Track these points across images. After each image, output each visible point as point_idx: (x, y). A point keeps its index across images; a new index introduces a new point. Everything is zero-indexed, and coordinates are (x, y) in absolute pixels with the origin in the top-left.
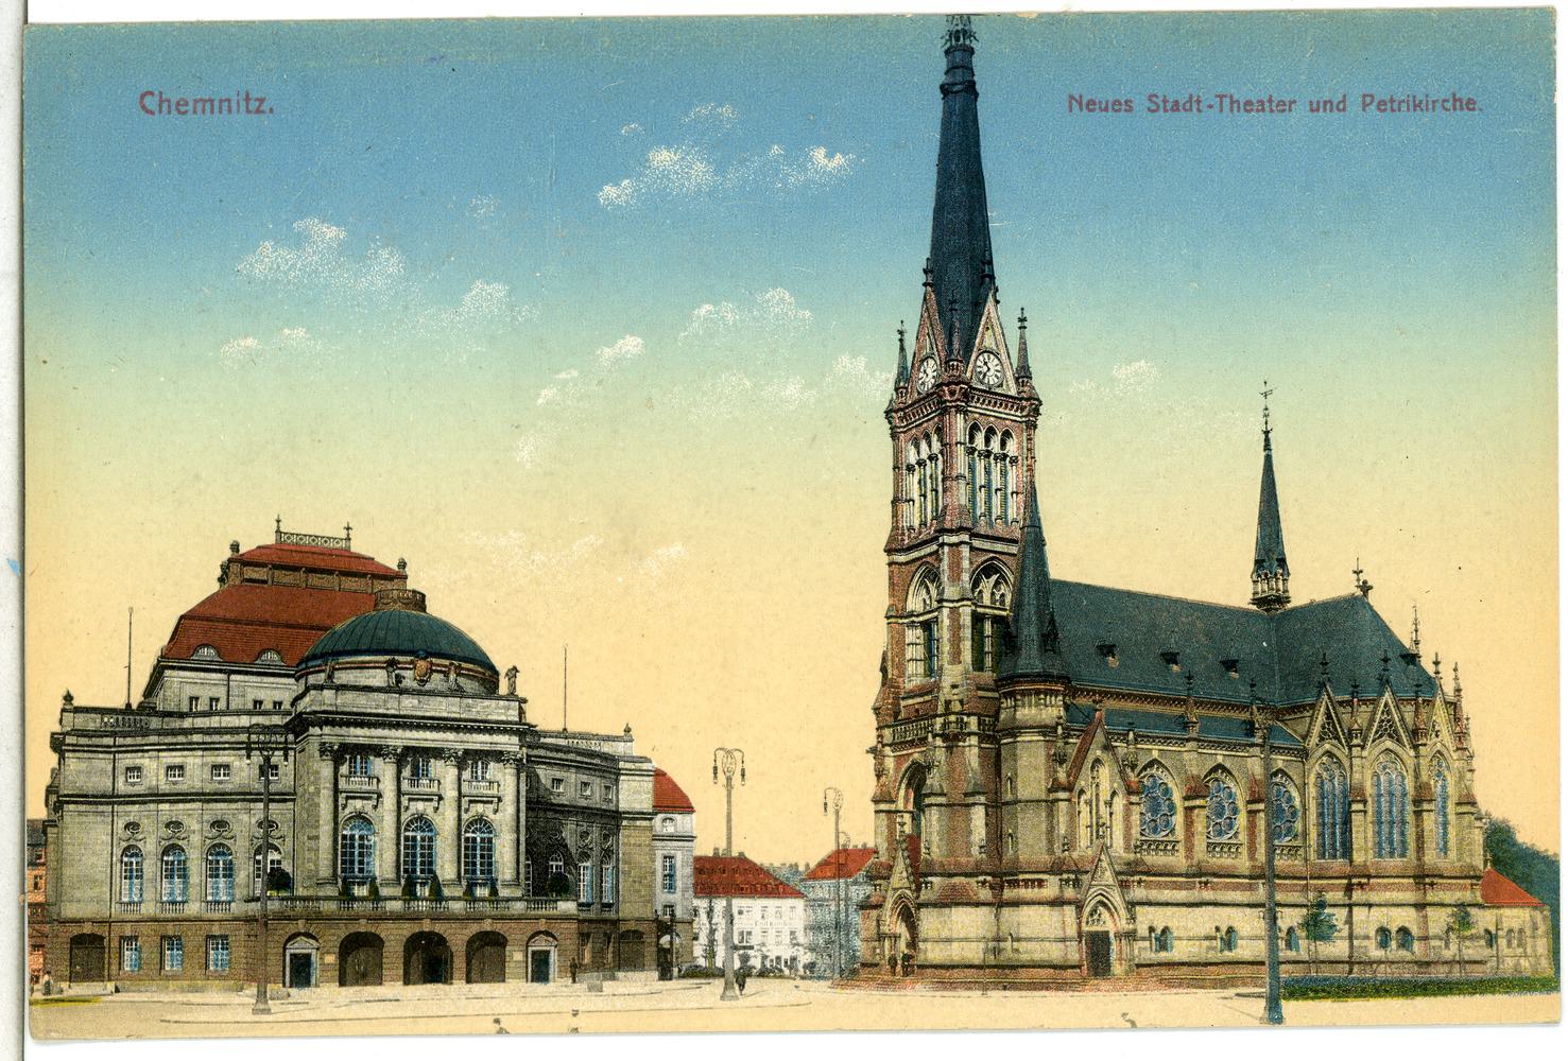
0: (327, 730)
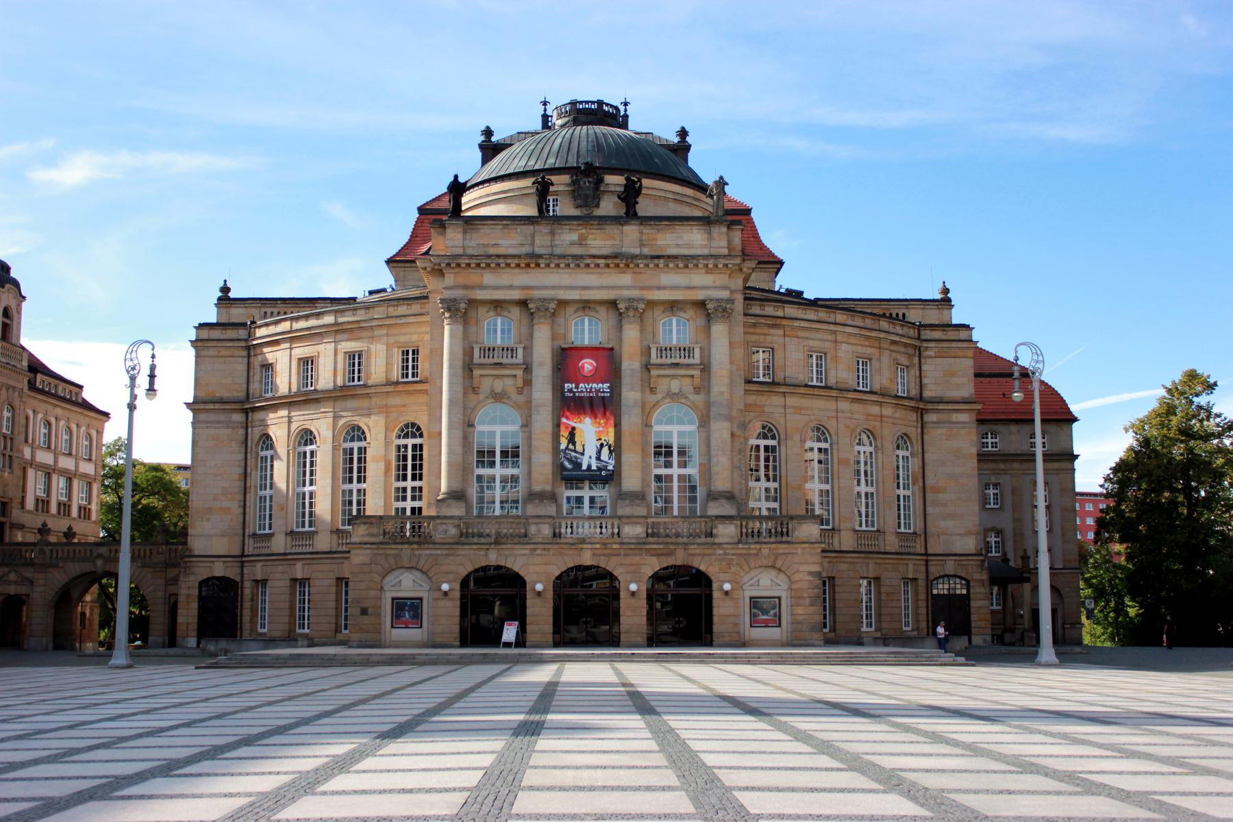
0: (450, 279)
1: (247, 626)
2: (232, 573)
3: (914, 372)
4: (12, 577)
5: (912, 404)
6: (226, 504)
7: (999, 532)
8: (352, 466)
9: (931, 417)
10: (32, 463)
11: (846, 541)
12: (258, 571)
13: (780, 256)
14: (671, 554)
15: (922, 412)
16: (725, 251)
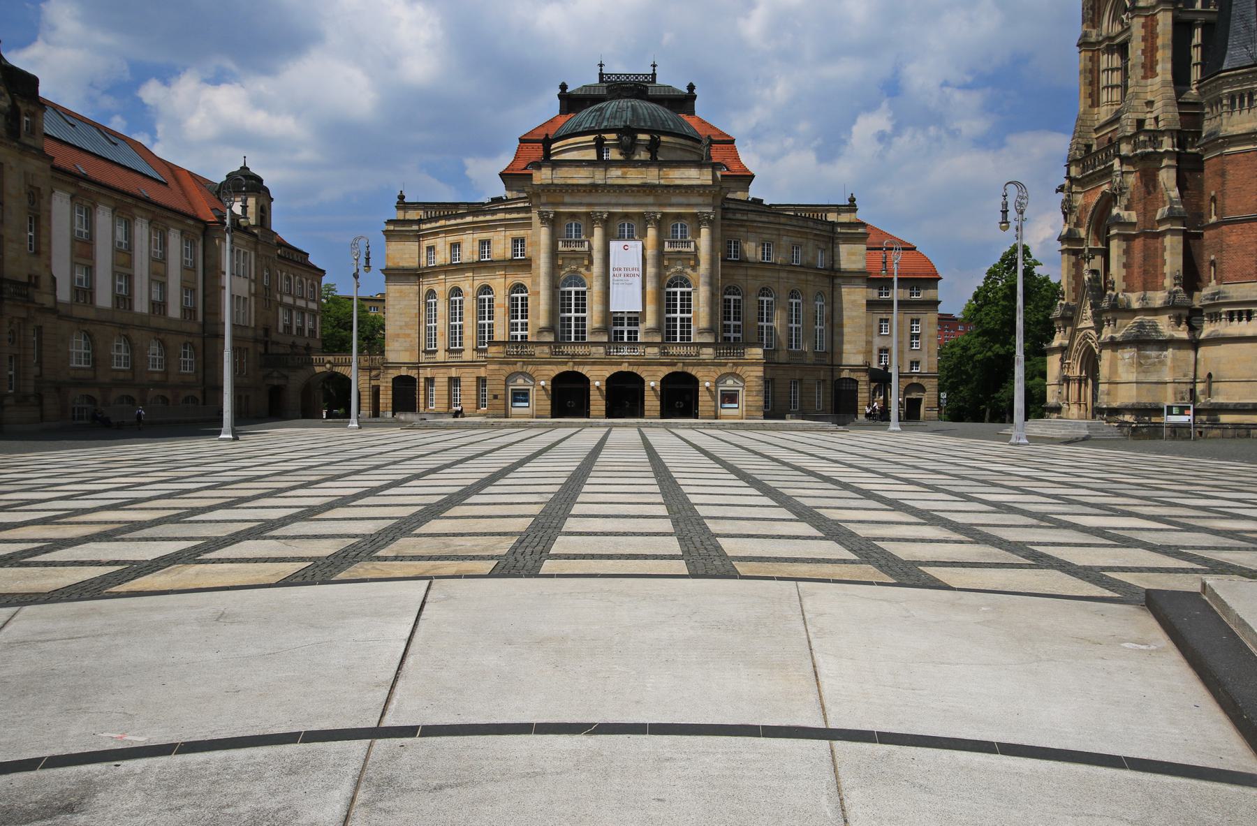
1: (422, 405)
2: (413, 373)
3: (829, 253)
4: (275, 374)
5: (827, 273)
6: (408, 331)
7: (887, 351)
8: (484, 309)
9: (838, 281)
10: (281, 304)
11: (782, 357)
12: (428, 373)
13: (752, 170)
14: (674, 364)
15: (833, 278)
16: (710, 182)
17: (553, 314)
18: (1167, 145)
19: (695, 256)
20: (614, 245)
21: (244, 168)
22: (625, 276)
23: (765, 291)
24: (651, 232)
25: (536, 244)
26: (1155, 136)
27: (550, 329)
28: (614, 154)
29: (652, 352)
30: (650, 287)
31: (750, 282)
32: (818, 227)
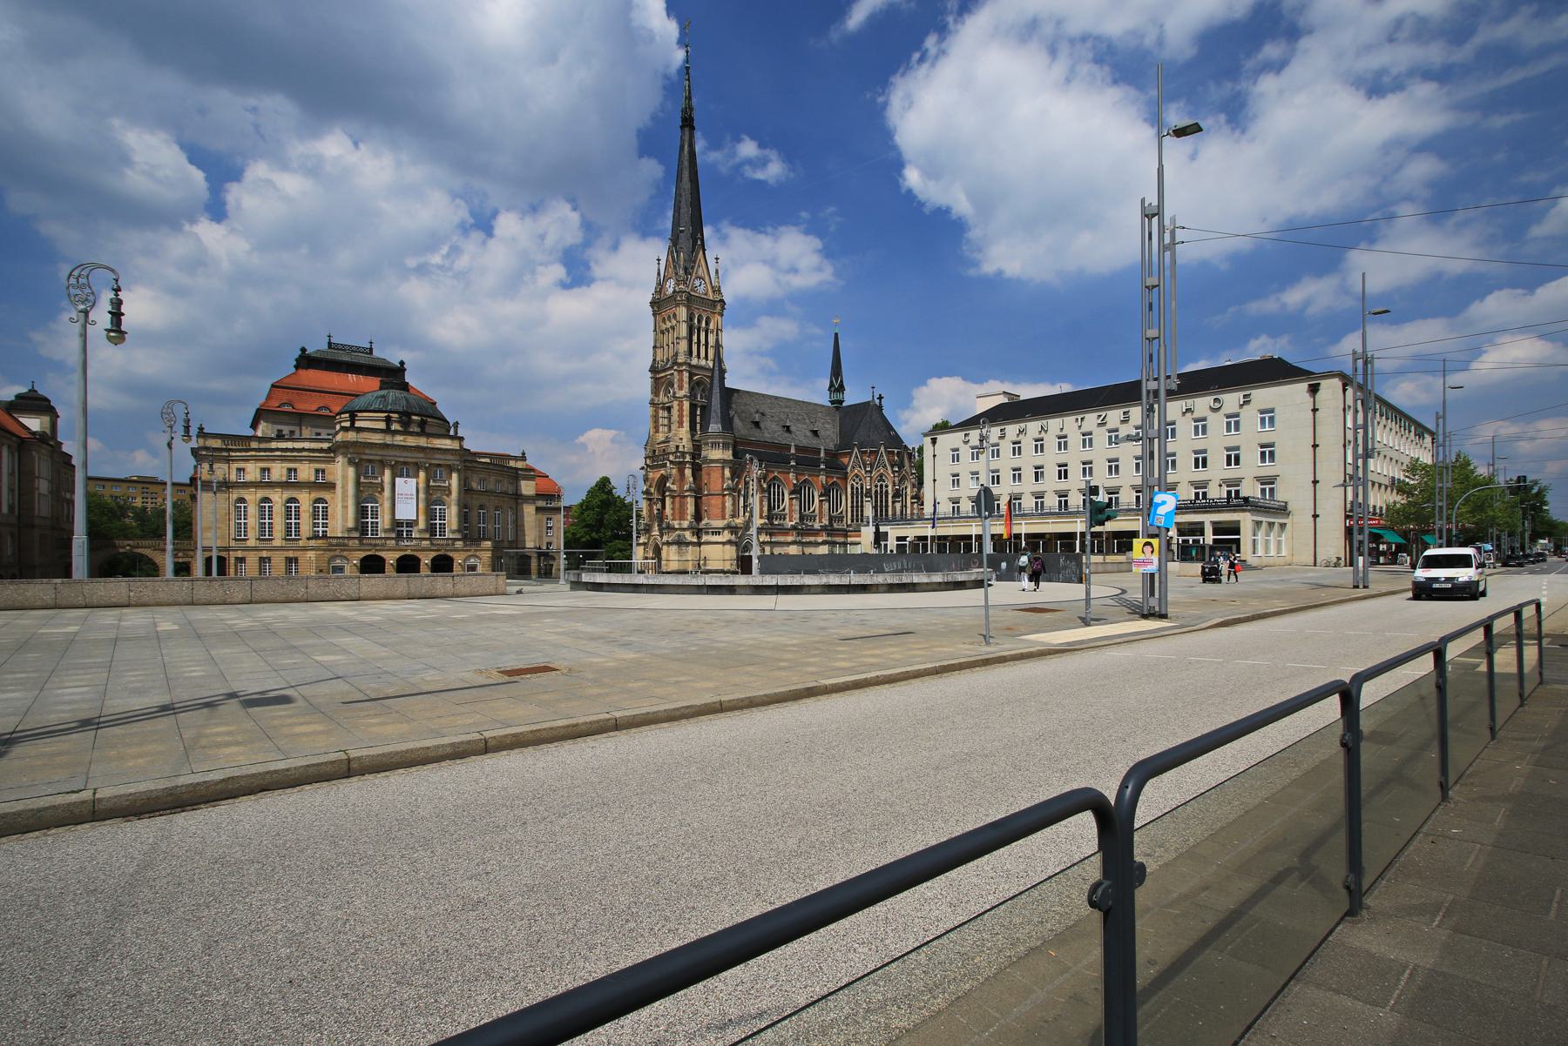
12: (240, 554)
17: (357, 520)
18: (688, 458)
19: (448, 491)
20: (398, 480)
21: (33, 391)
22: (406, 497)
23: (481, 507)
24: (422, 474)
25: (345, 477)
26: (683, 454)
27: (355, 529)
28: (395, 426)
29: (425, 543)
30: (421, 505)
31: (475, 502)
32: (506, 470)
